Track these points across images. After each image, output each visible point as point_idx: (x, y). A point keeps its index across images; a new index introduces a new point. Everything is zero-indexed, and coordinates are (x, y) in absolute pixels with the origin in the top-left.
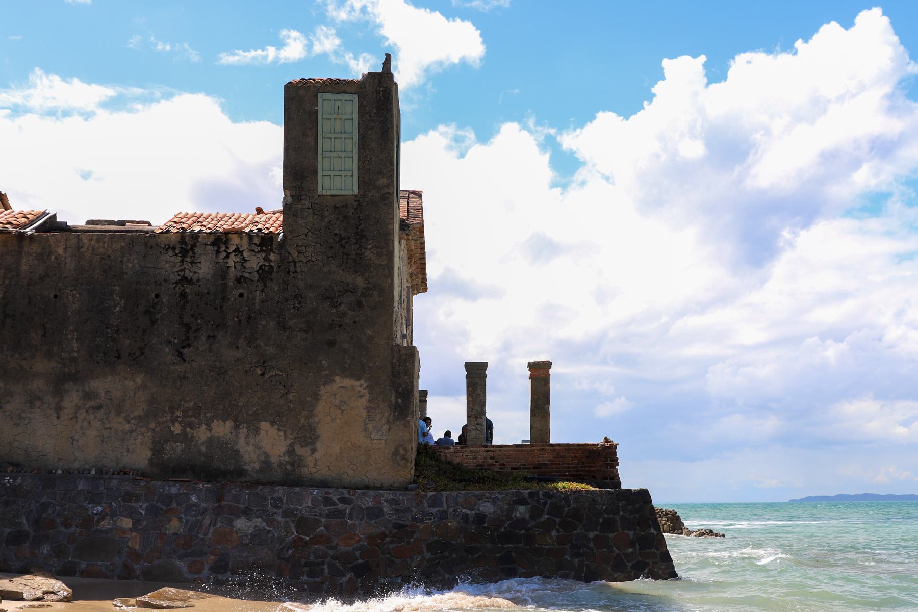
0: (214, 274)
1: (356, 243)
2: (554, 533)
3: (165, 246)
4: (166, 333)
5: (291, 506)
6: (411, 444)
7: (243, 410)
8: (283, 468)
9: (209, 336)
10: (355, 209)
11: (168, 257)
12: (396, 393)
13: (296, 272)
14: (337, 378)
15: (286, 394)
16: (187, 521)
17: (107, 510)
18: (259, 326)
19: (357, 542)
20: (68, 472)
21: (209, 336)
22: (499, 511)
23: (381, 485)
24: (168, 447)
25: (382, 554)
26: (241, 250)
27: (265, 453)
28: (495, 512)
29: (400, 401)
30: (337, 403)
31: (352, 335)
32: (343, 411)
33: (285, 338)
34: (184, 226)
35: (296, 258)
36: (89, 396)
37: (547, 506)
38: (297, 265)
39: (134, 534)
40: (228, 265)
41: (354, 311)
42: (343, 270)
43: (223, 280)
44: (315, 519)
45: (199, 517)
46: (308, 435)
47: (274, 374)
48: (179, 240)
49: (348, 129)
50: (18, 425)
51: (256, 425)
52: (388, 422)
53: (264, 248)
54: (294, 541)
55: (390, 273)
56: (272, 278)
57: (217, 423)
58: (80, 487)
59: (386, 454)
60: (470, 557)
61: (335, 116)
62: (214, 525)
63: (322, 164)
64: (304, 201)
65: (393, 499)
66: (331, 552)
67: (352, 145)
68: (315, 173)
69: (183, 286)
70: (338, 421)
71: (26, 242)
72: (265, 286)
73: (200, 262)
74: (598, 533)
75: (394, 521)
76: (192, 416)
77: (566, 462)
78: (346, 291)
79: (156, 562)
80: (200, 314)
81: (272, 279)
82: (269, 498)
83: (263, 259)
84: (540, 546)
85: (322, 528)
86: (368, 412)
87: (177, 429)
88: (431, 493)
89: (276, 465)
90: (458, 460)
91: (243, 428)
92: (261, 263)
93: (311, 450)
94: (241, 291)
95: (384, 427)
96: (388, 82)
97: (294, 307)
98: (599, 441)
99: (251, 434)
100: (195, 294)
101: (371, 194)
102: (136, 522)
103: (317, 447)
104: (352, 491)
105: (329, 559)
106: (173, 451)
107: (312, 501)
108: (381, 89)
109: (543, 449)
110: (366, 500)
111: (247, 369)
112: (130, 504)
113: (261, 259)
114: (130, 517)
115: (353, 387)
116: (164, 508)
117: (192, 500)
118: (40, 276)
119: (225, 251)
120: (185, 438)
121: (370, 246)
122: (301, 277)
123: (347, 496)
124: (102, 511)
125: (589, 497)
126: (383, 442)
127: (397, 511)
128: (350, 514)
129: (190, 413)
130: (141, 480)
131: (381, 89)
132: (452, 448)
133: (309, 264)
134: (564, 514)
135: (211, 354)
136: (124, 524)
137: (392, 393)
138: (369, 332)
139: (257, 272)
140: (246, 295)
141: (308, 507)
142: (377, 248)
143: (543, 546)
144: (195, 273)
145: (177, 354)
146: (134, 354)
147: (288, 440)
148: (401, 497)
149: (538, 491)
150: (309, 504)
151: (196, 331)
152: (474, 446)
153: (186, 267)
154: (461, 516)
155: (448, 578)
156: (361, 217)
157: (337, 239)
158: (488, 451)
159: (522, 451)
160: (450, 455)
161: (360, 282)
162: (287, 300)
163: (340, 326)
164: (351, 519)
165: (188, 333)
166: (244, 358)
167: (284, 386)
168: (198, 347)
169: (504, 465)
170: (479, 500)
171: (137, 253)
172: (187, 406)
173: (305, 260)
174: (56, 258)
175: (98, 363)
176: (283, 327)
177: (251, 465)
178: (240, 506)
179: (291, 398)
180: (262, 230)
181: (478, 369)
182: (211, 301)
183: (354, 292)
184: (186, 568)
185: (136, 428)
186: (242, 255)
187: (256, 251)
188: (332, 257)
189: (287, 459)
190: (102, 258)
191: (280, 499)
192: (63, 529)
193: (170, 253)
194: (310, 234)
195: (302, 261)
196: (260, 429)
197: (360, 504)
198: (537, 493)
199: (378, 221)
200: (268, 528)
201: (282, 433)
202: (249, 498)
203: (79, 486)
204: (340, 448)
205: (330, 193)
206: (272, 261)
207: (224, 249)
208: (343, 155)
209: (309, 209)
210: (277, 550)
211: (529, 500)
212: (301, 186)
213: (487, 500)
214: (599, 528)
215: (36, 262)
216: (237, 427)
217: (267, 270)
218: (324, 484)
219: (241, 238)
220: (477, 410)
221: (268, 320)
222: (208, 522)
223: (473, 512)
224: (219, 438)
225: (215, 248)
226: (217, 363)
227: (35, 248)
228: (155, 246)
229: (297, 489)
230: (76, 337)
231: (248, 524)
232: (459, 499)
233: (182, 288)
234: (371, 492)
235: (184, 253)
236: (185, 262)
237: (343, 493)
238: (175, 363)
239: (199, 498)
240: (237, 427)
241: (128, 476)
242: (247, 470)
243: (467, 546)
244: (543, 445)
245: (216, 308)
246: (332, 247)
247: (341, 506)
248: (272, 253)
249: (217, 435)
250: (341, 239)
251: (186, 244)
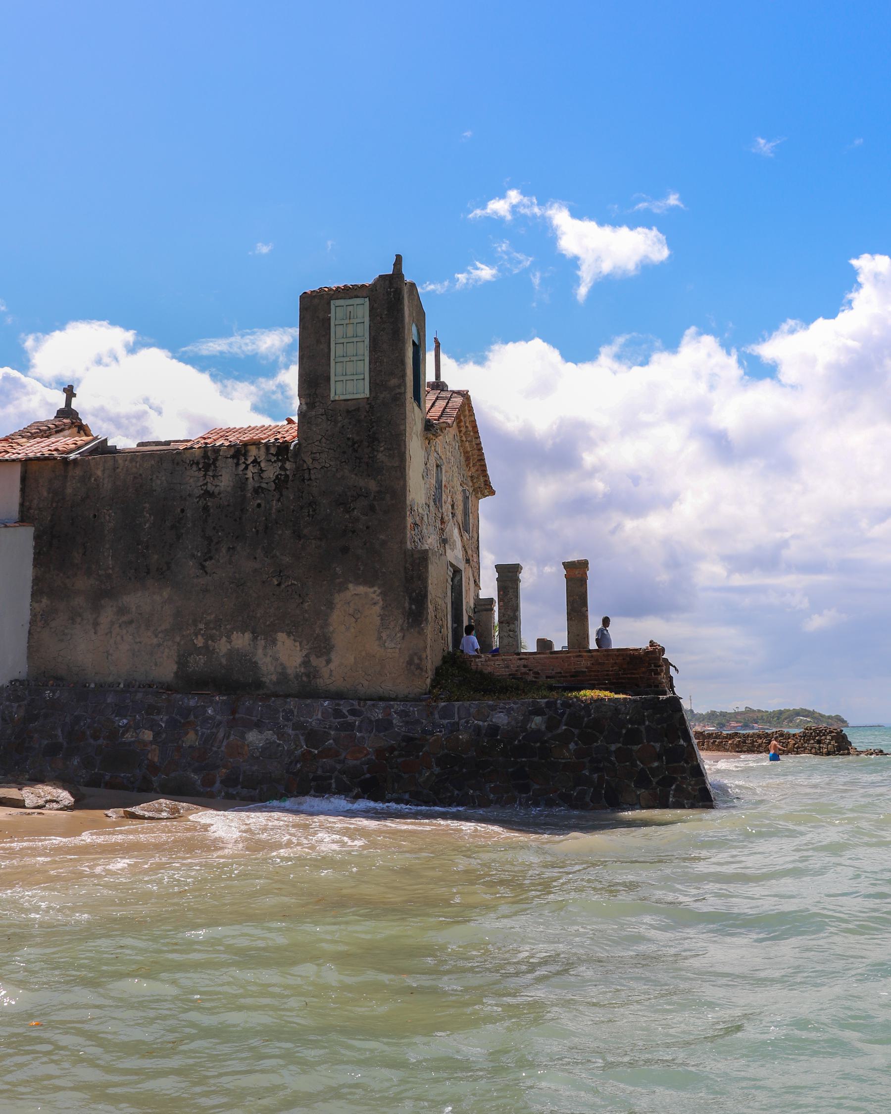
0: (234, 486)
1: (368, 447)
2: (572, 746)
3: (190, 462)
4: (190, 547)
5: (302, 719)
6: (426, 652)
7: (261, 621)
8: (299, 680)
9: (229, 548)
10: (368, 412)
11: (192, 472)
12: (410, 599)
13: (310, 479)
14: (351, 586)
15: (302, 603)
16: (203, 734)
17: (132, 723)
18: (276, 536)
19: (366, 755)
20: (100, 686)
21: (229, 548)
22: (513, 723)
23: (397, 696)
24: (191, 660)
25: (390, 768)
26: (259, 460)
27: (282, 664)
28: (508, 723)
29: (413, 607)
30: (351, 612)
31: (366, 540)
32: (357, 620)
33: (300, 546)
34: (208, 441)
35: (310, 465)
36: (122, 611)
37: (565, 716)
38: (312, 472)
39: (154, 746)
40: (247, 476)
41: (367, 516)
42: (356, 474)
43: (242, 491)
44: (325, 732)
45: (214, 730)
46: (322, 645)
48: (202, 455)
49: (360, 333)
50: (62, 641)
52: (402, 630)
53: (280, 458)
54: (303, 754)
55: (402, 474)
56: (288, 486)
58: (109, 700)
59: (401, 664)
60: (481, 771)
61: (347, 321)
62: (228, 738)
63: (335, 370)
64: (318, 408)
65: (403, 711)
66: (338, 767)
67: (364, 349)
68: (328, 379)
69: (205, 500)
70: (353, 630)
71: (71, 467)
72: (281, 495)
73: (221, 475)
74: (620, 745)
75: (403, 734)
76: (213, 629)
77: (606, 669)
78: (359, 496)
79: (173, 775)
80: (220, 526)
81: (287, 488)
82: (281, 710)
83: (280, 468)
84: (556, 760)
85: (331, 741)
86: (382, 619)
87: (200, 642)
88: (443, 704)
89: (292, 676)
90: (489, 669)
91: (261, 639)
92: (278, 473)
93: (326, 660)
94: (259, 501)
95: (398, 635)
96: (399, 282)
97: (309, 515)
98: (644, 645)
100: (216, 507)
101: (383, 396)
102: (157, 735)
103: (332, 657)
104: (362, 702)
105: (336, 773)
106: (198, 663)
107: (323, 713)
108: (392, 290)
109: (580, 656)
110: (376, 712)
111: (265, 580)
112: (151, 716)
113: (278, 468)
114: (151, 730)
115: (366, 594)
116: (182, 721)
117: (208, 713)
118: (82, 498)
119: (244, 463)
120: (207, 650)
121: (382, 449)
122: (315, 484)
123: (357, 707)
124: (127, 724)
125: (612, 706)
126: (397, 650)
127: (407, 723)
128: (359, 726)
129: (212, 625)
130: (164, 693)
131: (392, 290)
132: (483, 656)
133: (323, 471)
134: (584, 725)
135: (232, 566)
136: (146, 736)
137: (405, 599)
138: (382, 537)
139: (274, 481)
140: (263, 505)
141: (318, 719)
142: (389, 449)
143: (560, 760)
144: (216, 486)
145: (200, 567)
146: (161, 569)
147: (303, 651)
148: (411, 709)
149: (557, 700)
150: (320, 716)
151: (217, 543)
153: (209, 481)
154: (472, 728)
155: (457, 794)
156: (373, 420)
157: (350, 443)
158: (520, 659)
159: (557, 658)
160: (482, 664)
161: (373, 486)
162: (302, 508)
163: (354, 532)
164: (360, 731)
165: (210, 545)
166: (261, 569)
167: (300, 595)
168: (218, 559)
169: (538, 673)
170: (492, 711)
171: (165, 470)
172: (208, 618)
173: (319, 467)
174: (95, 480)
175: (130, 579)
176: (298, 535)
177: (269, 677)
178: (253, 718)
179: (306, 608)
180: (279, 439)
181: (509, 572)
182: (231, 513)
183: (367, 497)
184: (199, 781)
185: (163, 642)
186: (260, 466)
187: (273, 461)
188: (345, 462)
189: (303, 670)
190: (135, 478)
191: (291, 712)
192: (92, 741)
193: (195, 468)
194: (324, 440)
195: (315, 468)
197: (369, 716)
198: (555, 703)
199: (390, 423)
200: (278, 741)
201: (298, 644)
202: (262, 710)
203: (108, 699)
204: (355, 658)
205: (342, 397)
206: (287, 470)
207: (243, 460)
208: (355, 358)
209: (322, 415)
210: (287, 764)
211: (546, 710)
212: (315, 393)
213: (501, 710)
214: (621, 739)
215: (79, 485)
216: (255, 638)
217: (283, 479)
218: (338, 696)
219: (259, 449)
220: (509, 615)
221: (284, 529)
222: (222, 735)
223: (486, 723)
224: (238, 650)
225: (235, 461)
226: (237, 575)
227: (78, 472)
228: (182, 462)
229: (309, 701)
230: (111, 554)
231: (260, 737)
232: (472, 710)
233: (205, 502)
234: (382, 704)
235: (207, 467)
236: (207, 476)
237: (353, 705)
238: (198, 576)
239: (215, 711)
240: (255, 638)
241: (151, 689)
242: (265, 682)
243: (479, 760)
244: (580, 651)
245: (235, 520)
246: (344, 452)
247: (350, 718)
248: (287, 462)
249: (236, 647)
250: (354, 443)
251: (208, 458)
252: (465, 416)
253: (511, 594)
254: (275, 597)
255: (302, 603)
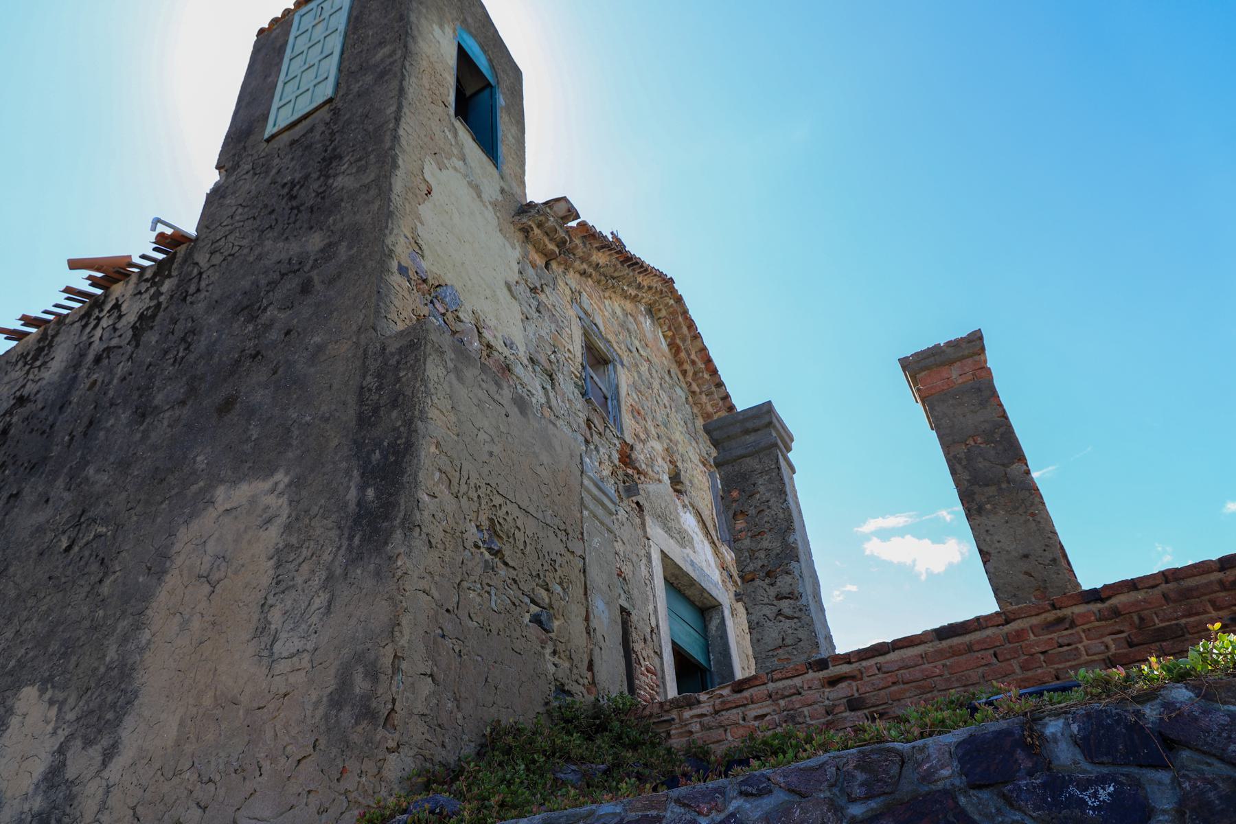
29: (370, 493)
95: (317, 602)
109: (1060, 621)
115: (253, 500)
149: (1034, 719)
152: (777, 675)
158: (833, 682)
159: (970, 648)
252: (684, 340)
253: (762, 489)
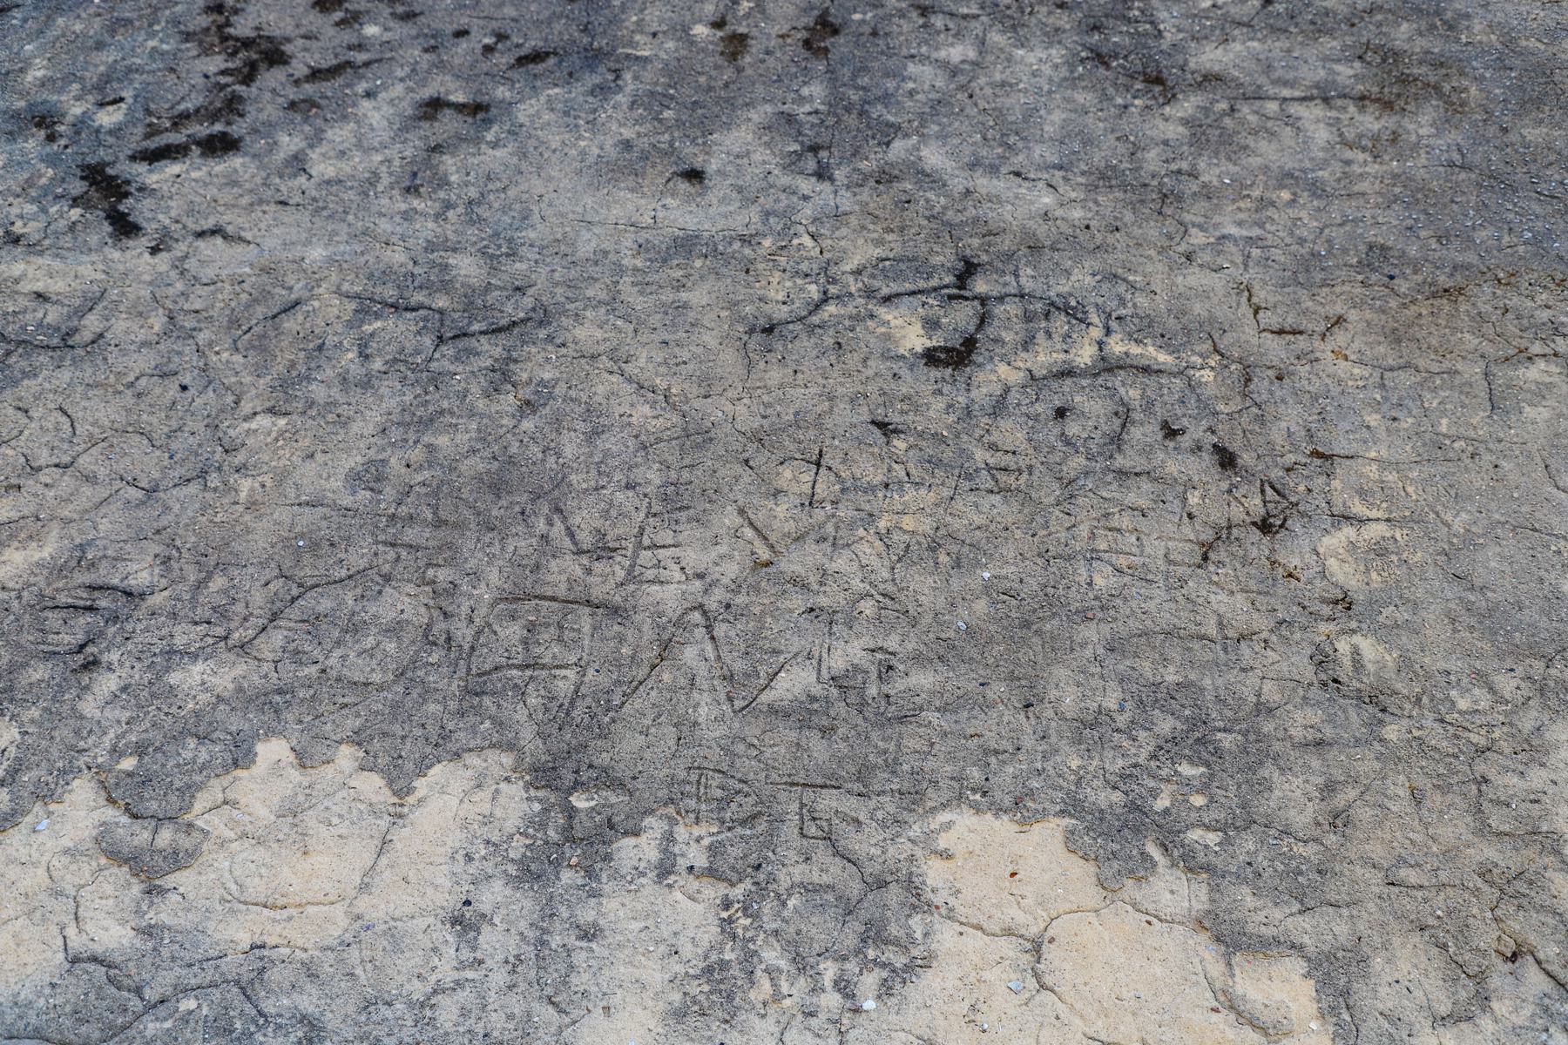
47: (1085, 355)
51: (864, 843)
57: (295, 775)
91: (665, 870)
99: (772, 955)
167: (1226, 460)
196: (917, 898)
254: (899, 444)
255: (1265, 526)
